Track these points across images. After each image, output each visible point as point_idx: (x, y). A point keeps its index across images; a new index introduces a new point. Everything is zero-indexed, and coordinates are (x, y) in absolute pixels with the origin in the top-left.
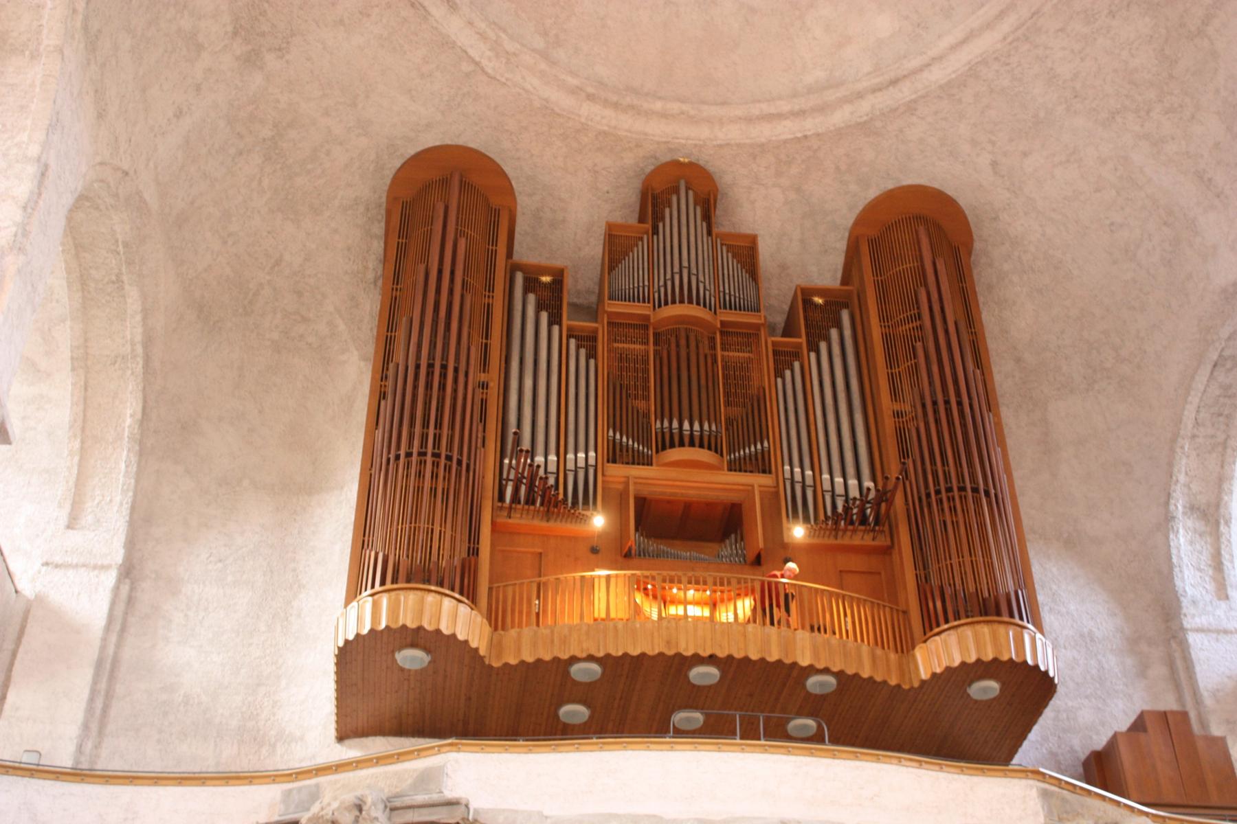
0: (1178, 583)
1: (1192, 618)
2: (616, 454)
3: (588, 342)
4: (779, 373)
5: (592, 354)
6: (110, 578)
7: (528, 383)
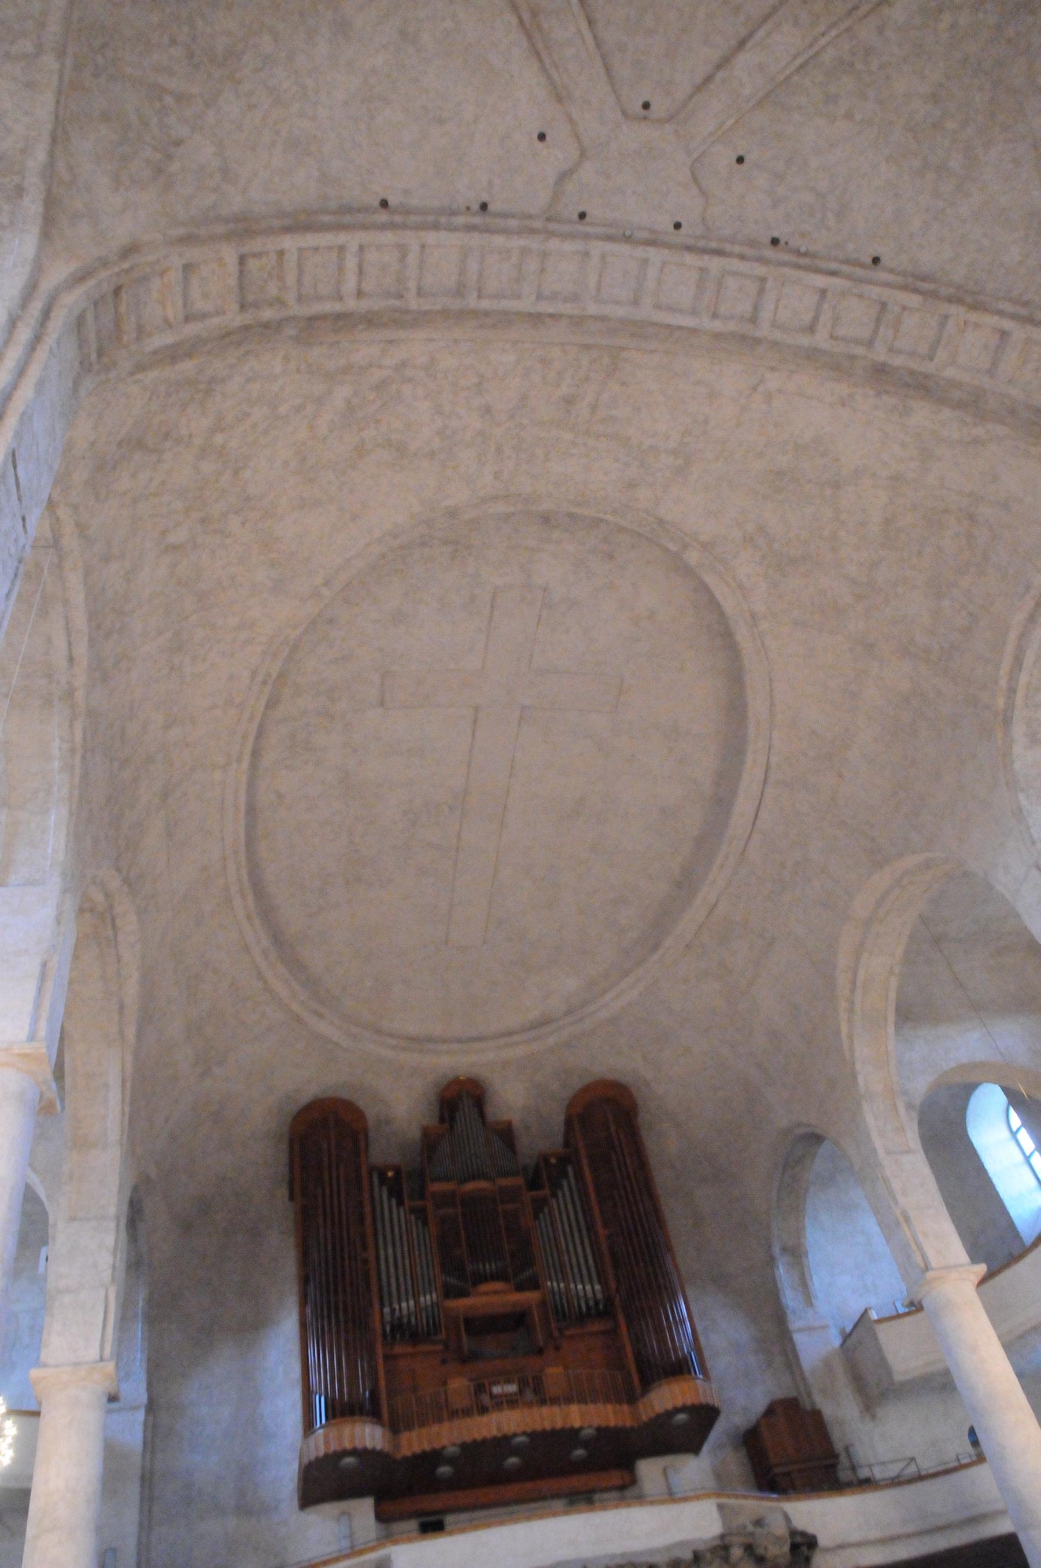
0: (784, 1301)
1: (795, 1323)
2: (449, 1292)
3: (421, 1214)
4: (536, 1217)
5: (425, 1223)
6: (140, 1415)
7: (390, 1251)
